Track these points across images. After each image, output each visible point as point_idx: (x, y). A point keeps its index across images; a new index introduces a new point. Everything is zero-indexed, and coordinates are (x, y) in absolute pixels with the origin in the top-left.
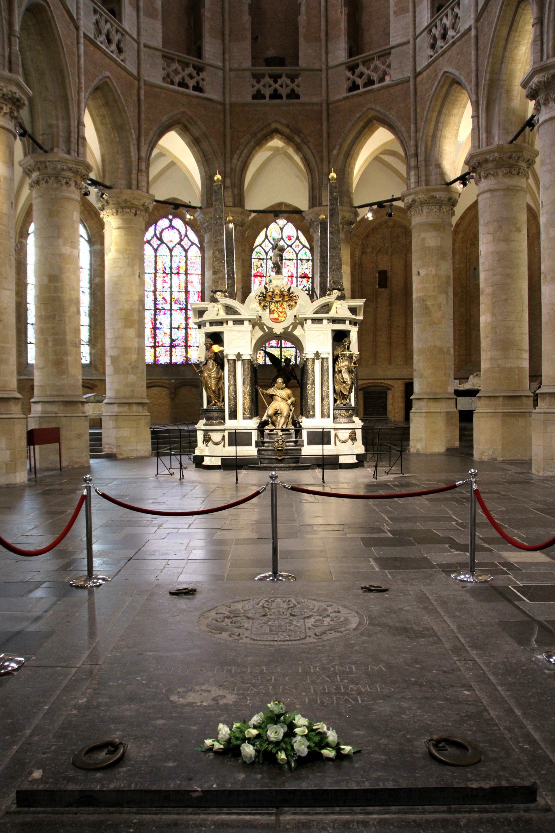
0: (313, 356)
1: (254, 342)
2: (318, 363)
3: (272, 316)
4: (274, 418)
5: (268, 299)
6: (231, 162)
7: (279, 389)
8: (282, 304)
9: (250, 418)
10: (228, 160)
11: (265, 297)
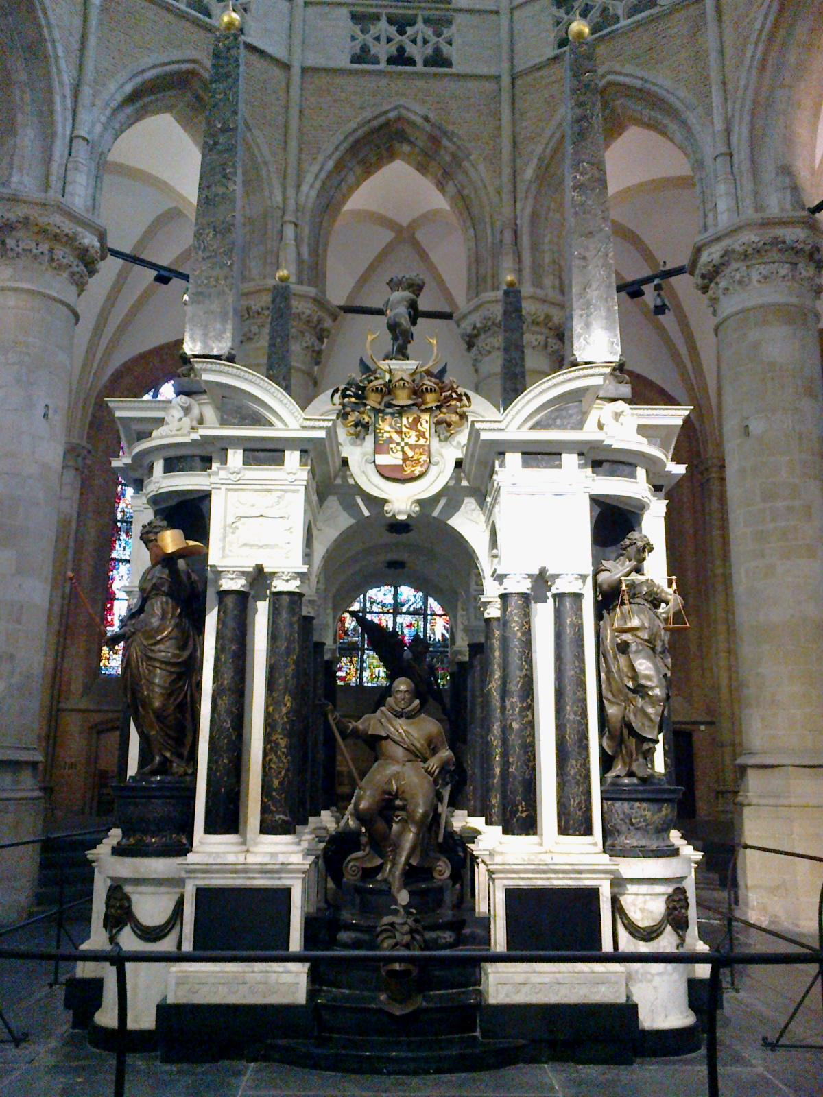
0: (525, 586)
1: (320, 551)
2: (543, 614)
3: (382, 459)
4: (380, 825)
5: (373, 400)
6: (298, 186)
7: (399, 715)
8: (417, 421)
9: (285, 829)
10: (291, 181)
11: (361, 397)
